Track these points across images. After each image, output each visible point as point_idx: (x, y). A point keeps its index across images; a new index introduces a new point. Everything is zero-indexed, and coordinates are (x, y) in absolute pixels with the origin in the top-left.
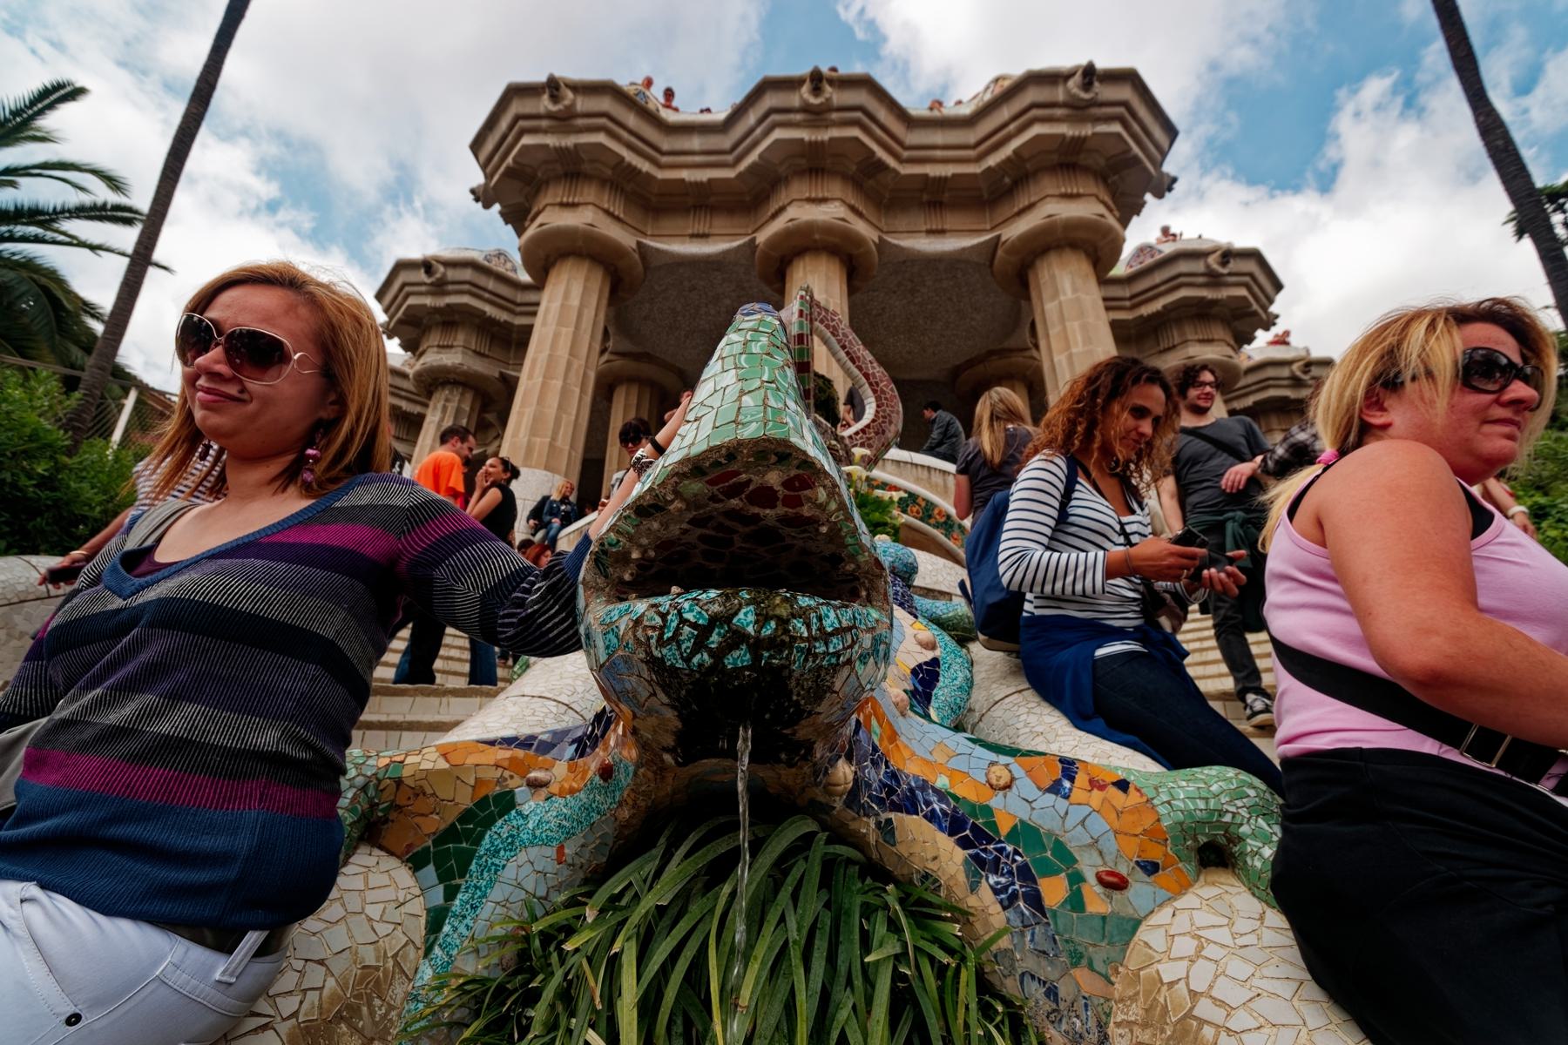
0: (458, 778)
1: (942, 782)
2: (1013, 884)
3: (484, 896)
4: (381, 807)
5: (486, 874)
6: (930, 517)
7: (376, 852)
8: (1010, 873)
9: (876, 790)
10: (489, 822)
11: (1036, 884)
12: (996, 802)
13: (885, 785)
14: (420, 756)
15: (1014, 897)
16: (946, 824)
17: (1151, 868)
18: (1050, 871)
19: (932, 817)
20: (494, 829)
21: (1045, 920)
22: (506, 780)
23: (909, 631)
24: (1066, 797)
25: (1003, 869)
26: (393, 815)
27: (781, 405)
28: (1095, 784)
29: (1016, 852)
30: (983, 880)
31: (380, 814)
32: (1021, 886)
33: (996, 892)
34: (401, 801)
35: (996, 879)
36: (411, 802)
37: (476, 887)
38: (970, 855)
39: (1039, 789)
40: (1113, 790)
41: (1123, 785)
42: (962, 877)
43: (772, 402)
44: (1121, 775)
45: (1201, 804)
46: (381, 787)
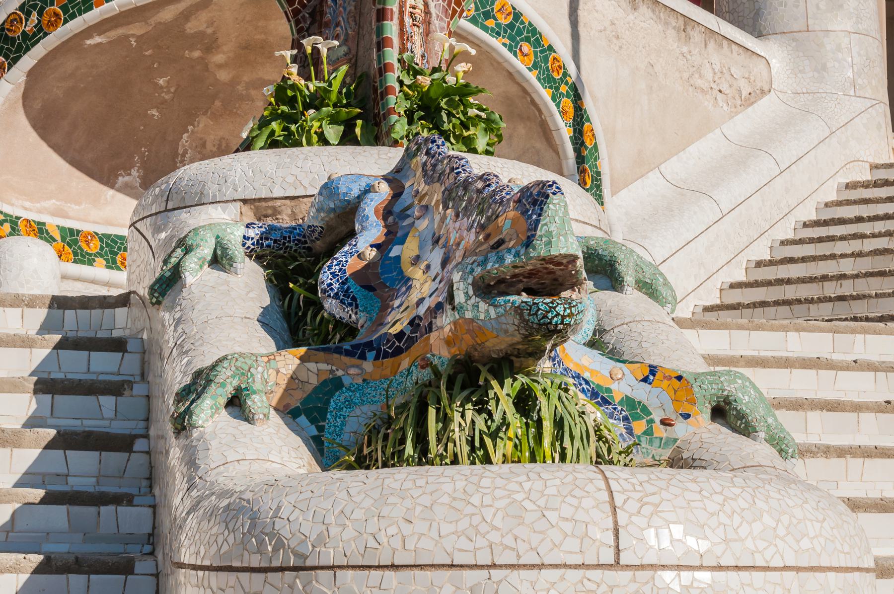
0: (308, 369)
1: (587, 375)
3: (342, 429)
5: (338, 420)
6: (487, 15)
8: (619, 419)
10: (331, 394)
12: (614, 386)
16: (589, 395)
18: (637, 418)
20: (335, 398)
22: (334, 371)
24: (650, 384)
28: (665, 377)
29: (622, 410)
37: (335, 426)
39: (637, 380)
40: (675, 380)
41: (679, 378)
44: (679, 373)
45: (715, 387)
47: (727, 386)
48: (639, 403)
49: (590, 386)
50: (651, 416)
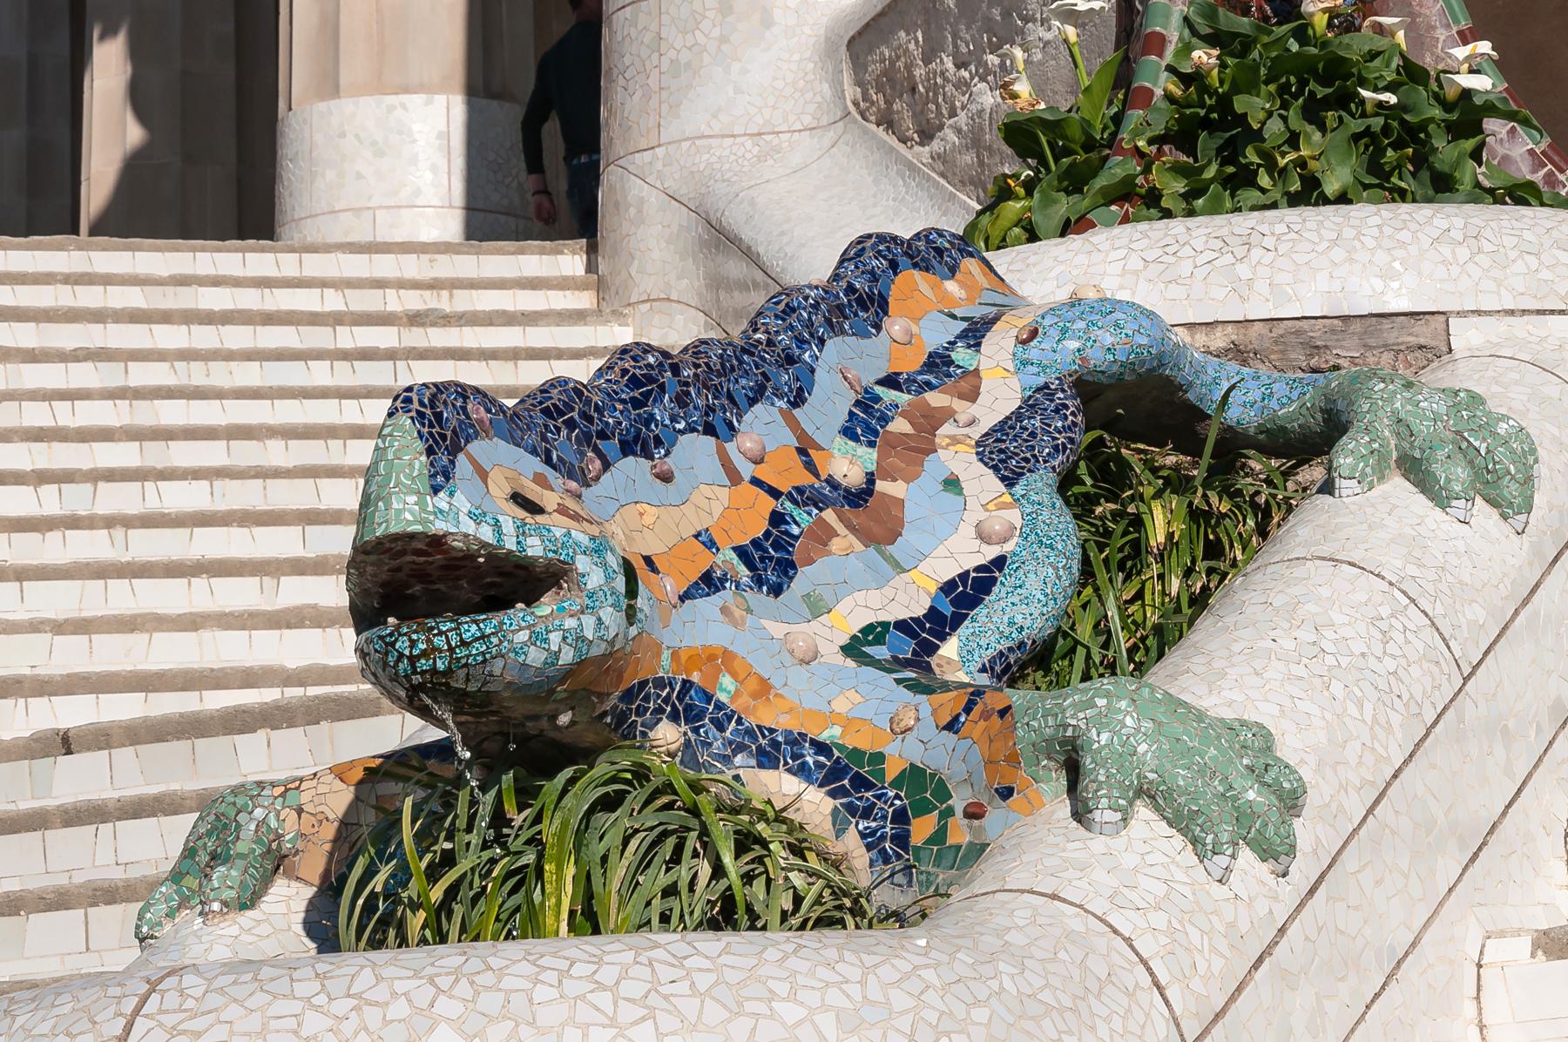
1: (830, 734)
2: (884, 827)
4: (287, 838)
7: (294, 884)
9: (719, 748)
11: (908, 822)
12: (891, 749)
13: (731, 743)
14: (316, 780)
15: (883, 837)
17: (1006, 793)
18: (923, 809)
19: (802, 771)
21: (907, 857)
23: (974, 514)
24: (956, 733)
25: (877, 814)
26: (300, 845)
27: (401, 506)
29: (897, 797)
30: (853, 826)
31: (289, 846)
32: (892, 829)
33: (863, 836)
34: (307, 830)
35: (866, 825)
36: (316, 829)
38: (841, 804)
39: (937, 727)
42: (828, 825)
43: (395, 505)
46: (281, 818)
47: (1072, 717)
48: (933, 776)
49: (829, 754)
50: (950, 802)
